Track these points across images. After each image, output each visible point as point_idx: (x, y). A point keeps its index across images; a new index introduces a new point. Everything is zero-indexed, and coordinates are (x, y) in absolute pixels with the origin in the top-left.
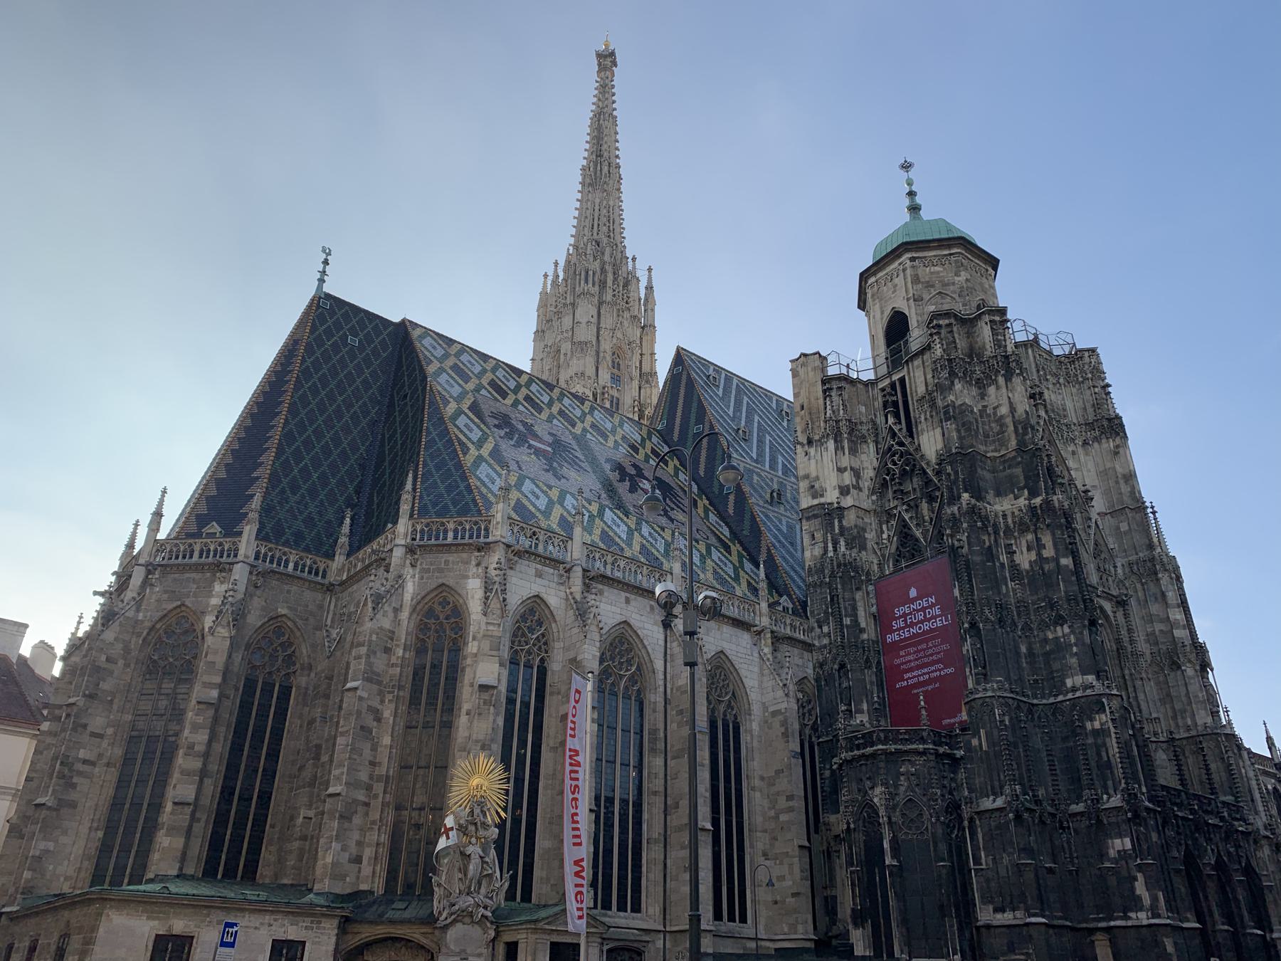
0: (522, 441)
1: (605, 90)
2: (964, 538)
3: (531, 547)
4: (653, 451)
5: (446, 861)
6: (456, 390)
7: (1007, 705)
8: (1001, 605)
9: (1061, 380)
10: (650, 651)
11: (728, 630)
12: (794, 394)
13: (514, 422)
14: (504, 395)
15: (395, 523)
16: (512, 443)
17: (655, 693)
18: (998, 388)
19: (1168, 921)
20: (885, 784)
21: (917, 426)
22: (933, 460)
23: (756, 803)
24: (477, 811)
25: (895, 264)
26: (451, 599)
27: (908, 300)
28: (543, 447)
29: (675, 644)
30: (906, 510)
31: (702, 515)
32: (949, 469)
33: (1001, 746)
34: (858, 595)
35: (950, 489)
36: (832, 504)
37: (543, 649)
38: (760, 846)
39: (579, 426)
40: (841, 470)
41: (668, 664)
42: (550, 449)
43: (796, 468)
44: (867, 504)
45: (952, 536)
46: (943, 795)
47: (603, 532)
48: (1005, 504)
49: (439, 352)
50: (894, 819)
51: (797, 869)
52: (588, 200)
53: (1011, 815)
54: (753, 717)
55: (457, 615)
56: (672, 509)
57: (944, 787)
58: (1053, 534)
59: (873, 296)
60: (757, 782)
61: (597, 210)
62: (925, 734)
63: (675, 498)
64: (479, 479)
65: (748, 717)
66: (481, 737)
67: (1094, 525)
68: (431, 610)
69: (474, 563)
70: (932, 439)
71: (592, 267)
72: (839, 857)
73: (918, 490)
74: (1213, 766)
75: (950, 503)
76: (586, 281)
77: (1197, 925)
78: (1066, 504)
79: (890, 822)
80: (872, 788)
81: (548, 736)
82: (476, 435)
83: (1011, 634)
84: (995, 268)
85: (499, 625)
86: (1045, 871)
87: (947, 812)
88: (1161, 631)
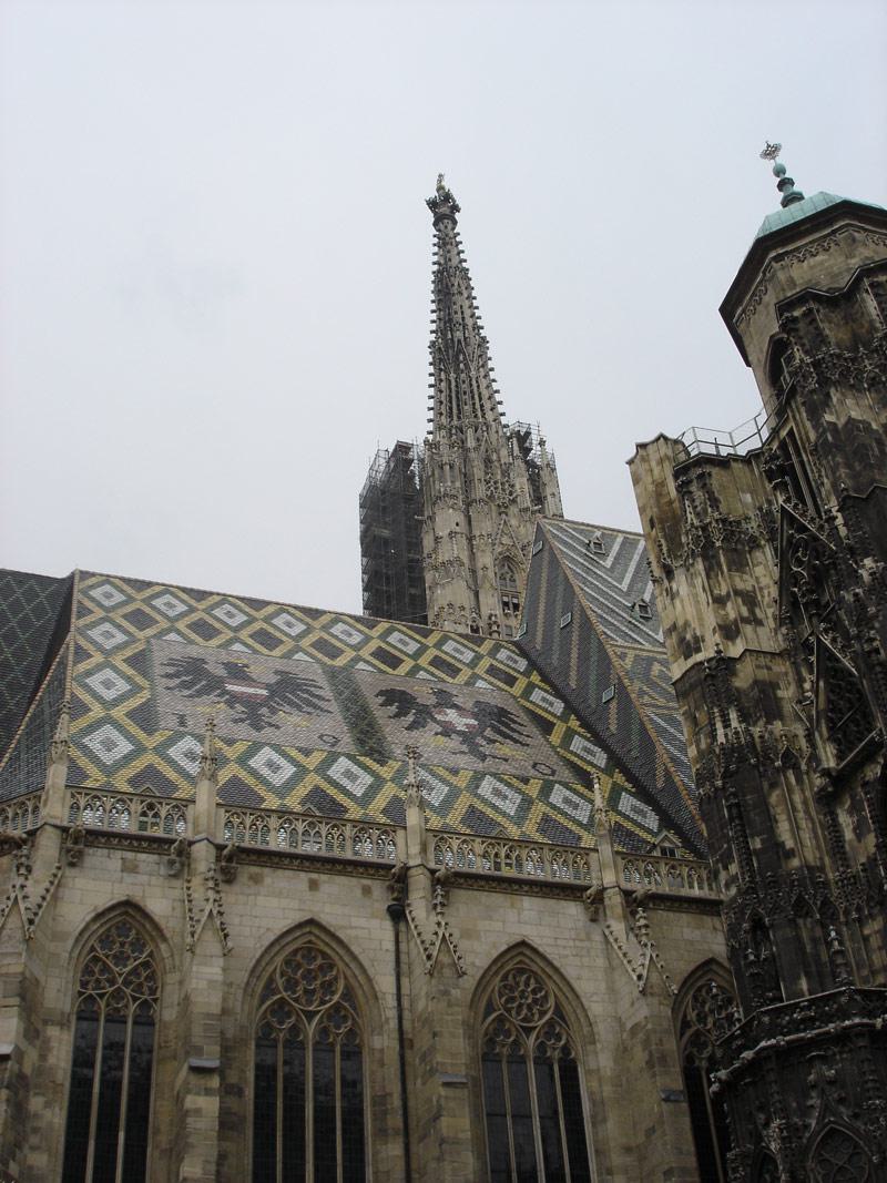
1: (447, 241)
10: (366, 964)
11: (530, 905)
12: (639, 508)
16: (187, 692)
17: (380, 1034)
20: (785, 1112)
34: (774, 798)
37: (145, 989)
40: (720, 601)
41: (405, 981)
42: (265, 692)
45: (858, 637)
52: (441, 381)
54: (599, 1046)
56: (494, 742)
60: (617, 1159)
63: (508, 726)
65: (590, 1048)
71: (445, 459)
80: (767, 1125)
81: (157, 1131)
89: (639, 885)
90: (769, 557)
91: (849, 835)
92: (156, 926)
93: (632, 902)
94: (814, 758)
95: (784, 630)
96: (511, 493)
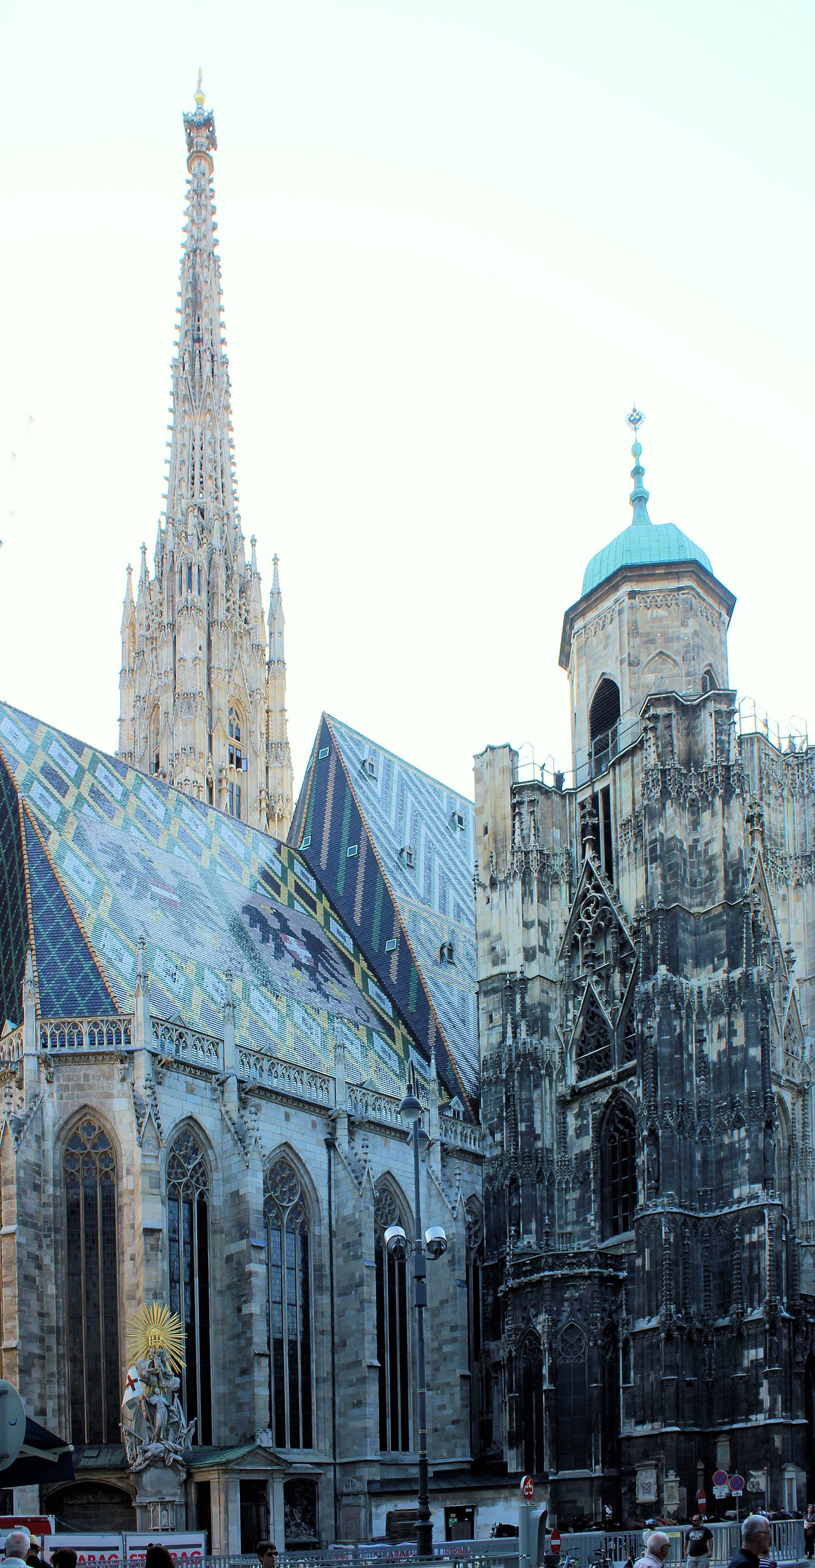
7: (674, 1221)
8: (682, 1106)
18: (713, 815)
30: (597, 982)
32: (648, 929)
33: (663, 1266)
35: (646, 958)
36: (515, 973)
44: (553, 974)
46: (602, 1319)
62: (592, 1257)
72: (497, 1383)
73: (611, 955)
75: (646, 978)
76: (190, 586)
83: (689, 1139)
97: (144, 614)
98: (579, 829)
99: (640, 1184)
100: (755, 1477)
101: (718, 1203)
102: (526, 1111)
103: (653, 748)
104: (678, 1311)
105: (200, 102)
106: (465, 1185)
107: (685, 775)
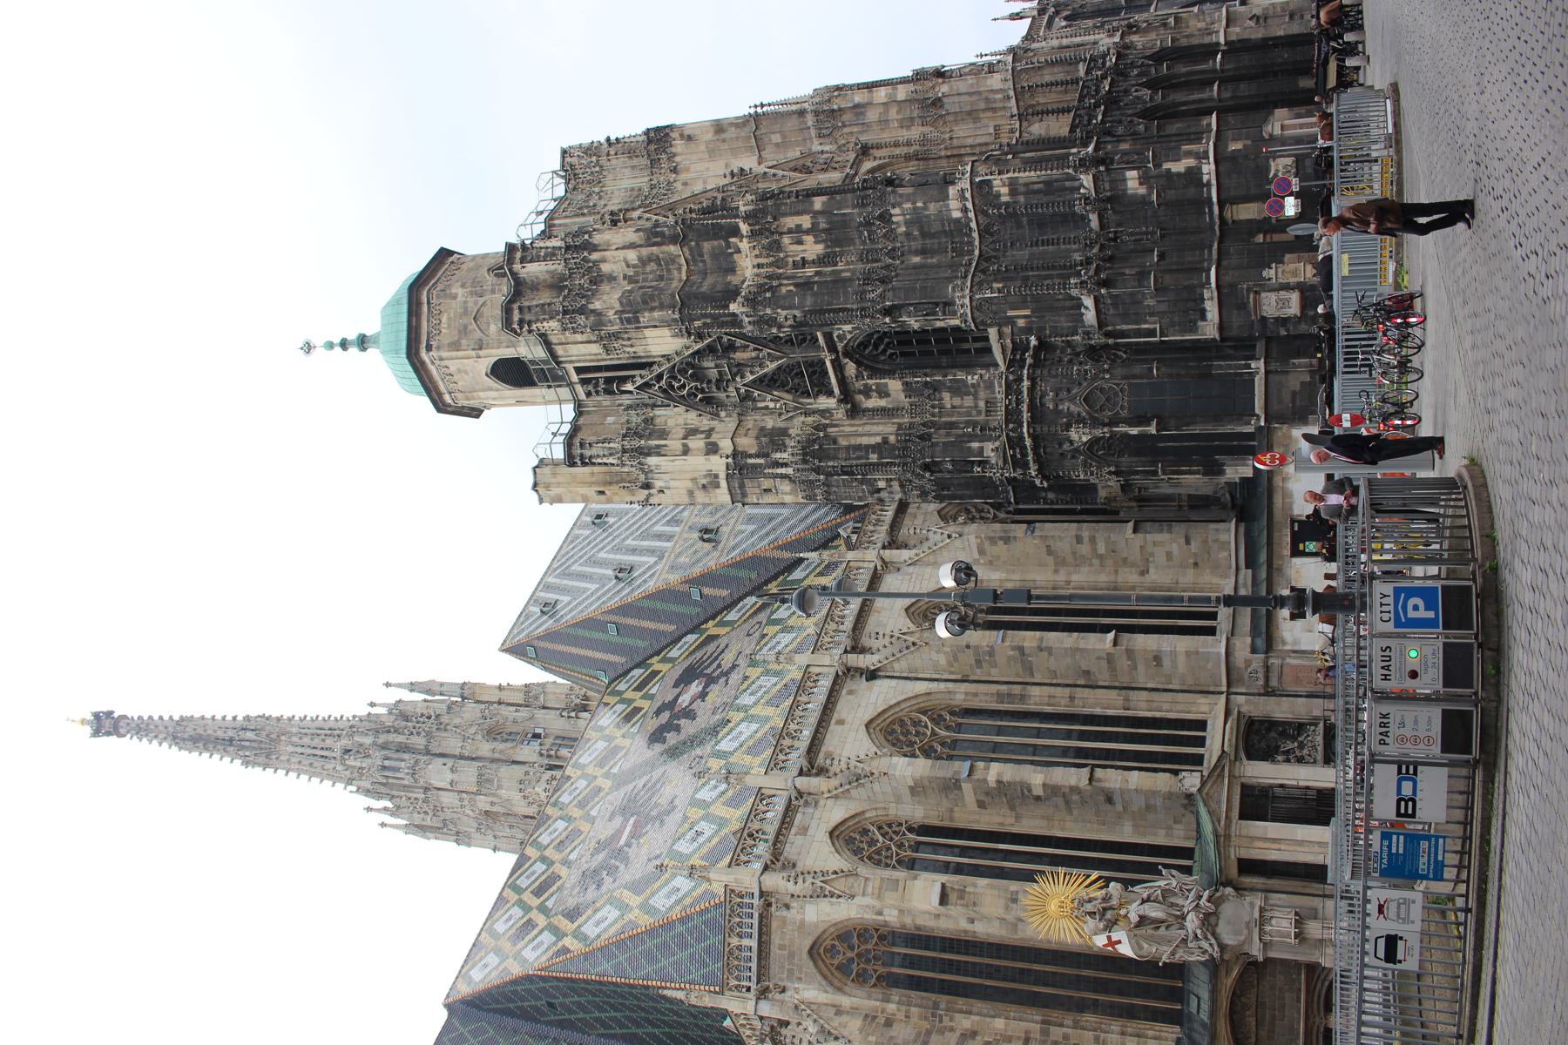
0: (620, 854)
2: (784, 313)
3: (766, 841)
4: (639, 688)
5: (1146, 946)
6: (547, 938)
7: (980, 283)
9: (597, 190)
13: (594, 865)
14: (556, 877)
15: (724, 1014)
16: (622, 867)
17: (955, 693)
19: (1211, 143)
20: (1068, 426)
21: (639, 357)
22: (685, 341)
23: (1084, 579)
24: (1089, 907)
25: (432, 368)
26: (828, 942)
27: (479, 357)
28: (628, 829)
29: (896, 666)
30: (742, 377)
31: (727, 629)
32: (697, 324)
34: (843, 442)
36: (728, 465)
38: (1130, 577)
39: (600, 782)
40: (686, 451)
41: (920, 676)
43: (677, 505)
44: (731, 424)
47: (749, 751)
48: (744, 265)
49: (493, 960)
50: (1106, 420)
51: (1159, 537)
53: (1103, 291)
55: (848, 935)
56: (719, 666)
57: (1070, 361)
58: (785, 215)
59: (468, 399)
60: (1061, 577)
61: (303, 750)
62: (1011, 377)
64: (672, 907)
66: (1002, 902)
67: (773, 171)
68: (839, 968)
69: (784, 913)
70: (656, 341)
74: (1048, 78)
75: (740, 324)
77: (1214, 115)
78: (749, 197)
79: (1110, 424)
80: (1071, 442)
81: (1001, 824)
82: (611, 913)
84: (450, 253)
85: (867, 879)
86: (1162, 263)
87: (1097, 361)
88: (898, 112)
89: (881, 534)
90: (665, 413)
91: (883, 403)
92: (853, 817)
93: (892, 544)
94: (824, 413)
95: (723, 414)
96: (429, 718)
97: (416, 815)
98: (608, 397)
99: (939, 324)
100: (1277, 171)
101: (966, 234)
102: (858, 453)
103: (545, 324)
104: (1078, 274)
105: (83, 722)
106: (927, 524)
107: (570, 290)
